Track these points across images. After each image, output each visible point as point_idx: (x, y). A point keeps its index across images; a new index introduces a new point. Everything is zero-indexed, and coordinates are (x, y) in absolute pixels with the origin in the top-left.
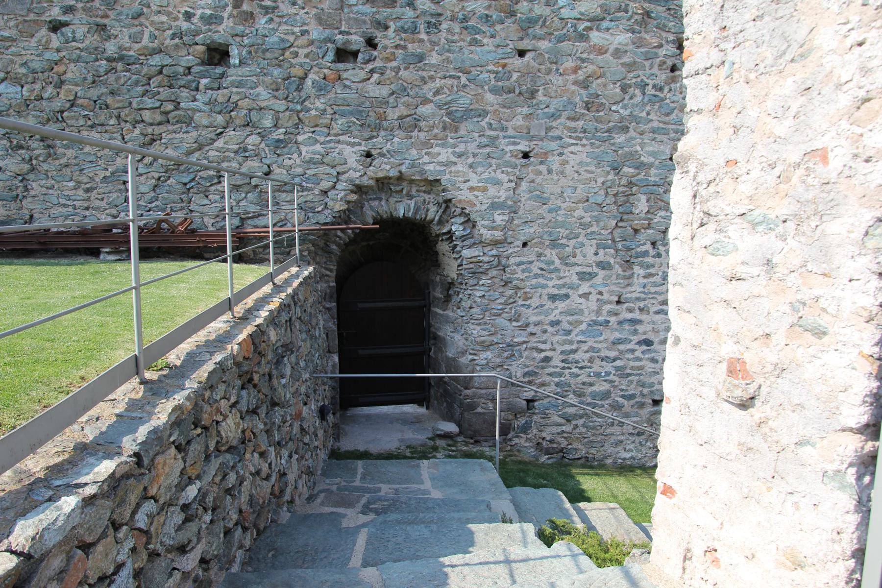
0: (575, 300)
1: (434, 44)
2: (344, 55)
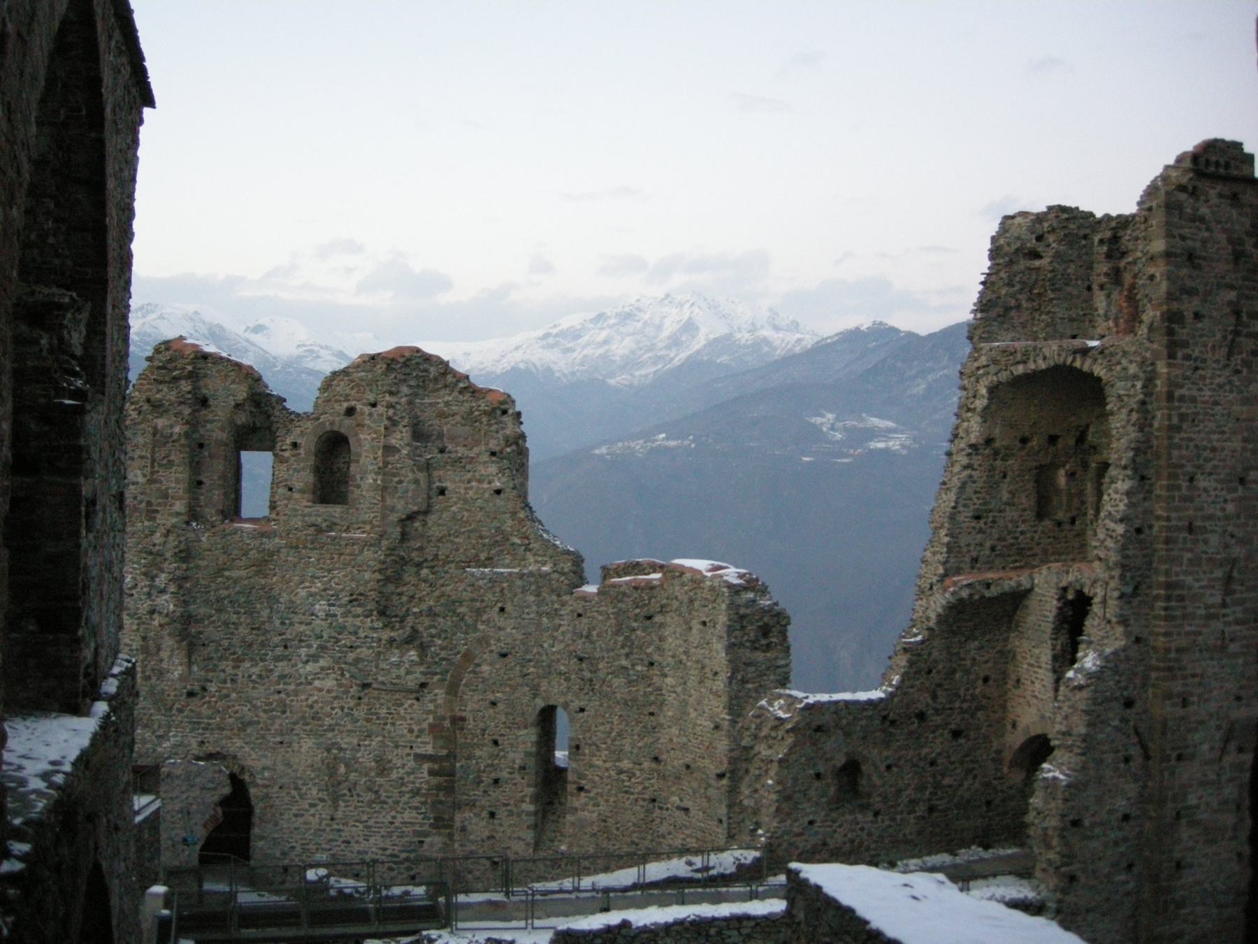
2: (191, 694)
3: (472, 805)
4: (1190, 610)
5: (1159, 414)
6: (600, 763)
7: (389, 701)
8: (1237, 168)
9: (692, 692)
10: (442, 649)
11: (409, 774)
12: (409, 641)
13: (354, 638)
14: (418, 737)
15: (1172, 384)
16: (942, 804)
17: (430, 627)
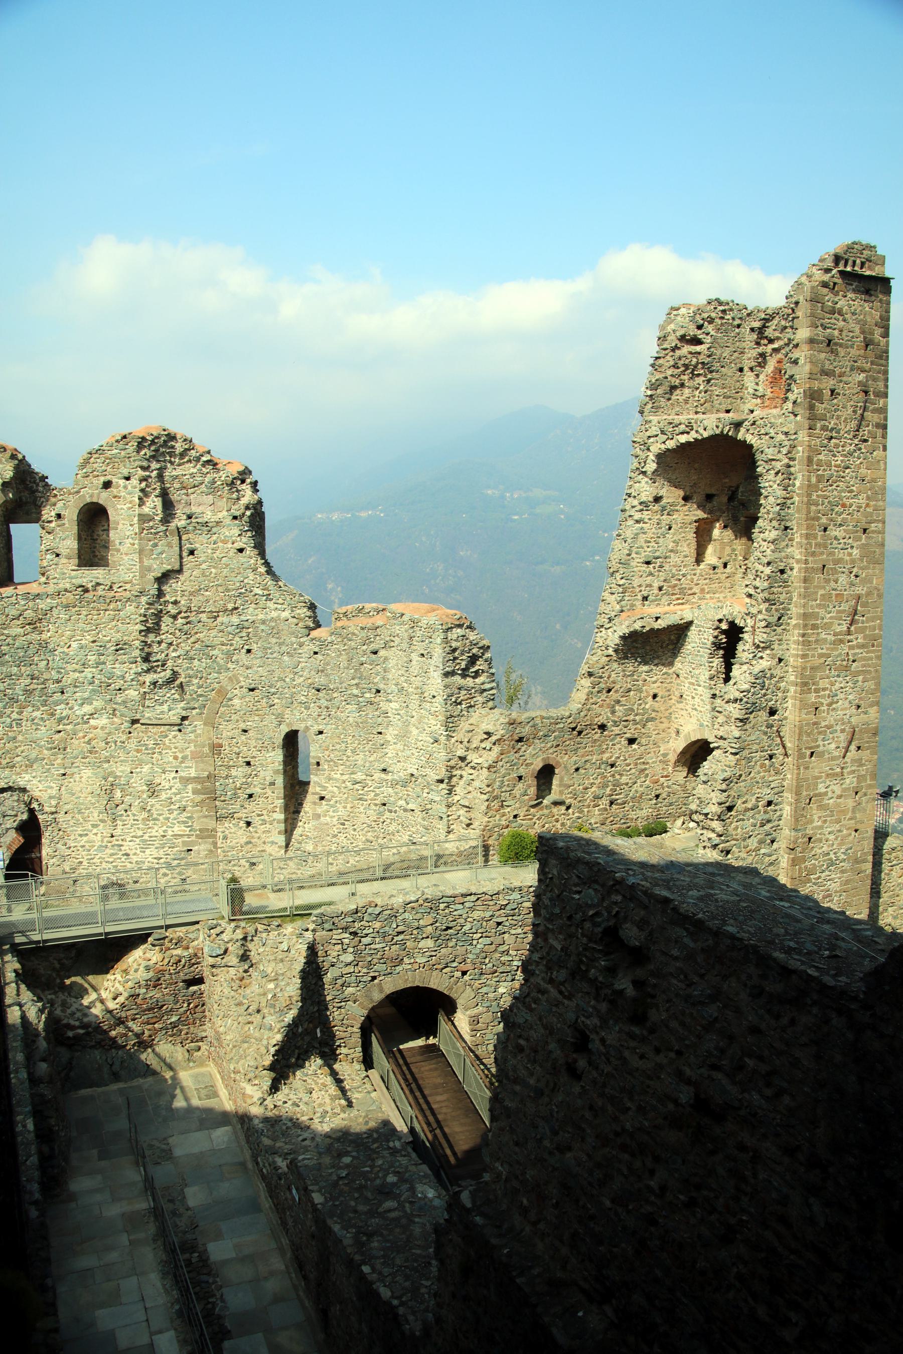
0: (91, 836)
1: (20, 732)
3: (232, 816)
4: (823, 636)
5: (800, 476)
6: (338, 776)
7: (155, 734)
8: (870, 268)
9: (414, 714)
10: (201, 687)
11: (176, 794)
12: (170, 681)
13: (122, 682)
14: (182, 762)
15: (813, 451)
16: (621, 798)
17: (188, 668)
